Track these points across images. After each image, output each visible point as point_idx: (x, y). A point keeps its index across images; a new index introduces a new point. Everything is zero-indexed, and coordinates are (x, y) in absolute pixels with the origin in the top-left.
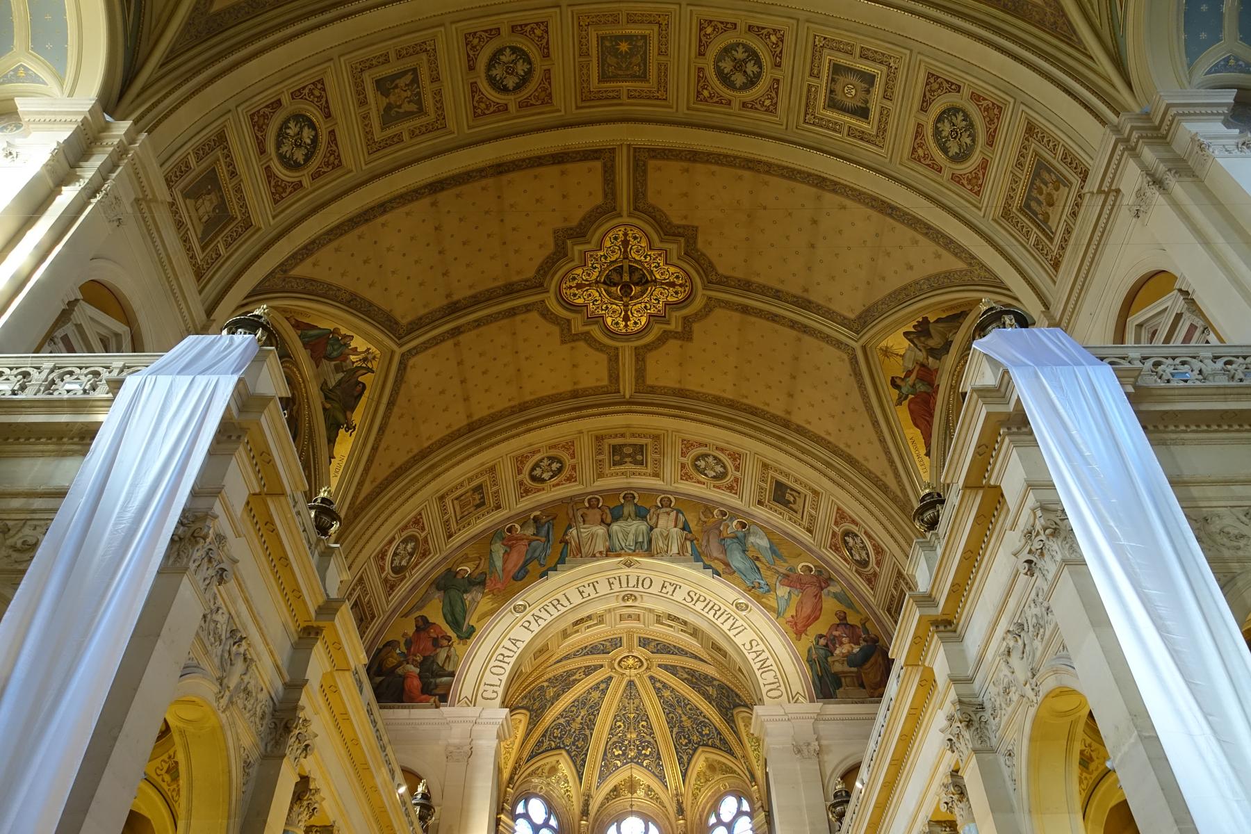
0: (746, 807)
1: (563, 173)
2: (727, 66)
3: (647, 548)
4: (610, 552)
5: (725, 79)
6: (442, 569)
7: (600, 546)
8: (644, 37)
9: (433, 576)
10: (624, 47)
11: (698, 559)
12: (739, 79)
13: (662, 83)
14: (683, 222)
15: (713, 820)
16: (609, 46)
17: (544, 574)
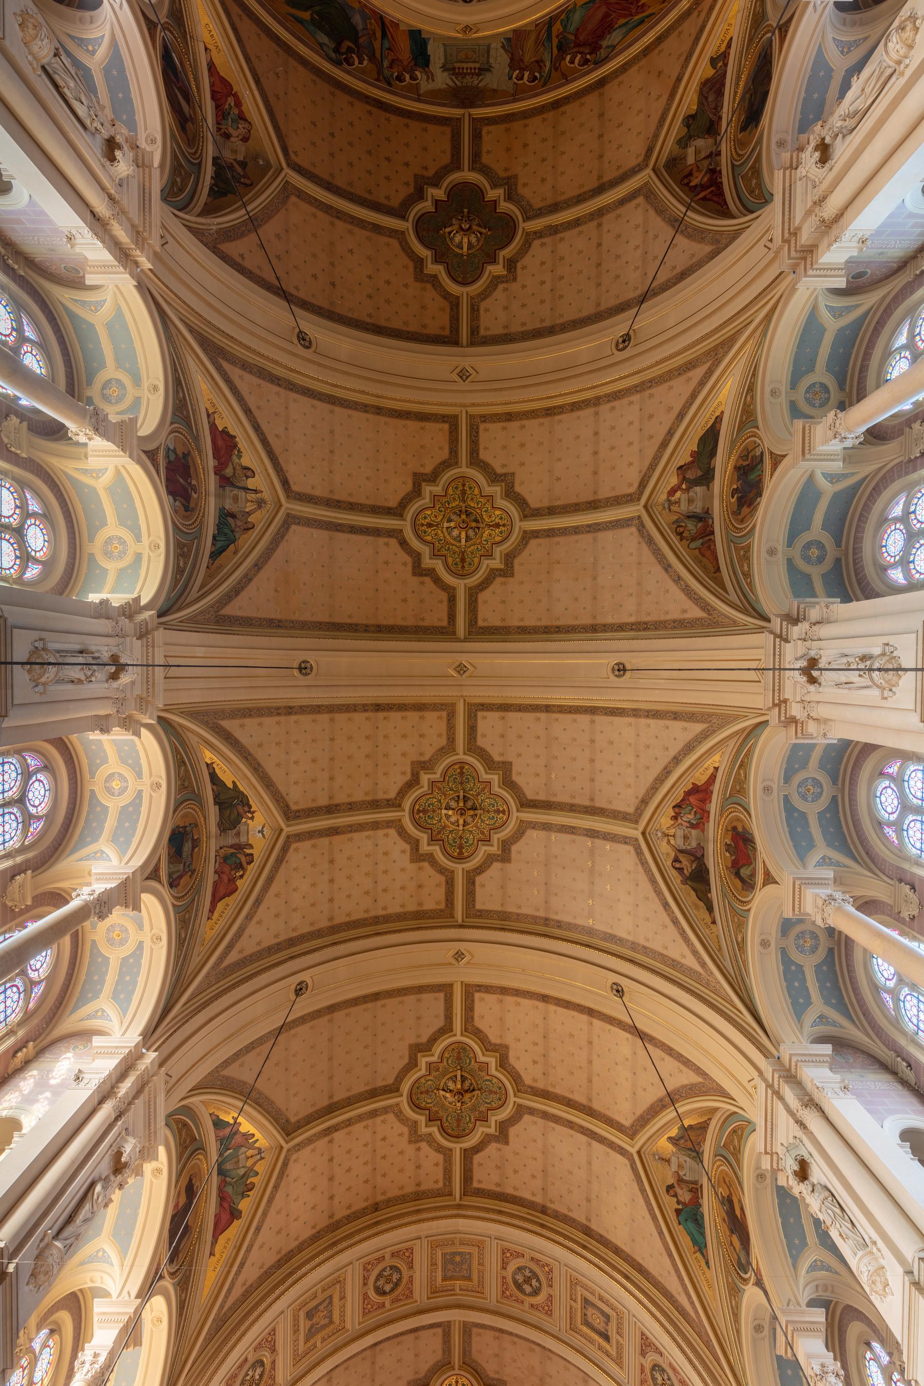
1: (416, 1338)
2: (520, 1278)
5: (519, 1287)
8: (470, 1254)
10: (458, 1259)
12: (528, 1289)
13: (481, 1282)
14: (496, 1376)
16: (449, 1259)
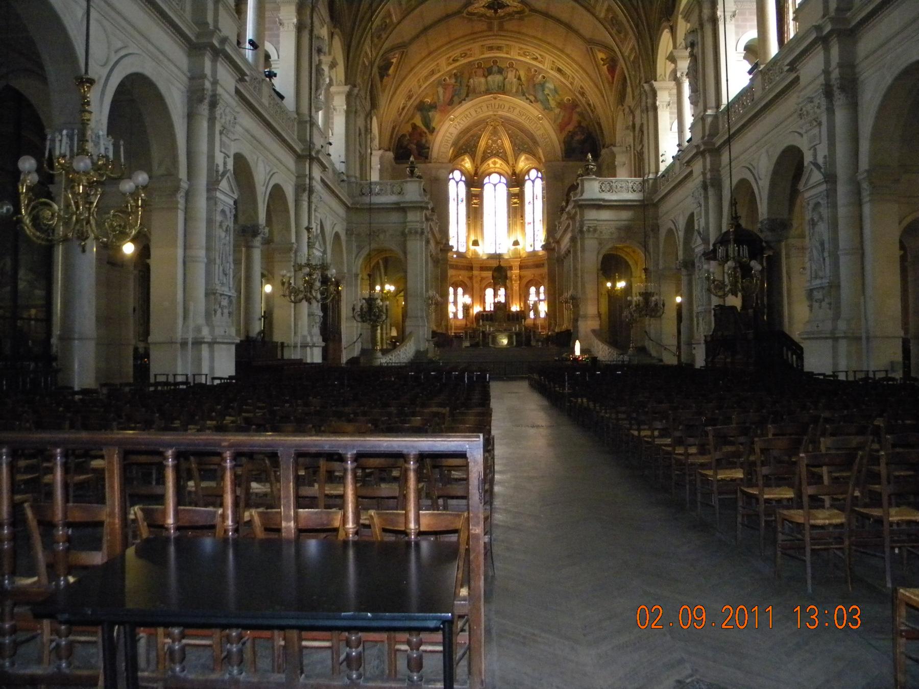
0: (540, 175)
3: (502, 89)
4: (488, 92)
6: (418, 100)
7: (483, 88)
9: (416, 103)
11: (524, 95)
15: (527, 177)
17: (460, 102)
